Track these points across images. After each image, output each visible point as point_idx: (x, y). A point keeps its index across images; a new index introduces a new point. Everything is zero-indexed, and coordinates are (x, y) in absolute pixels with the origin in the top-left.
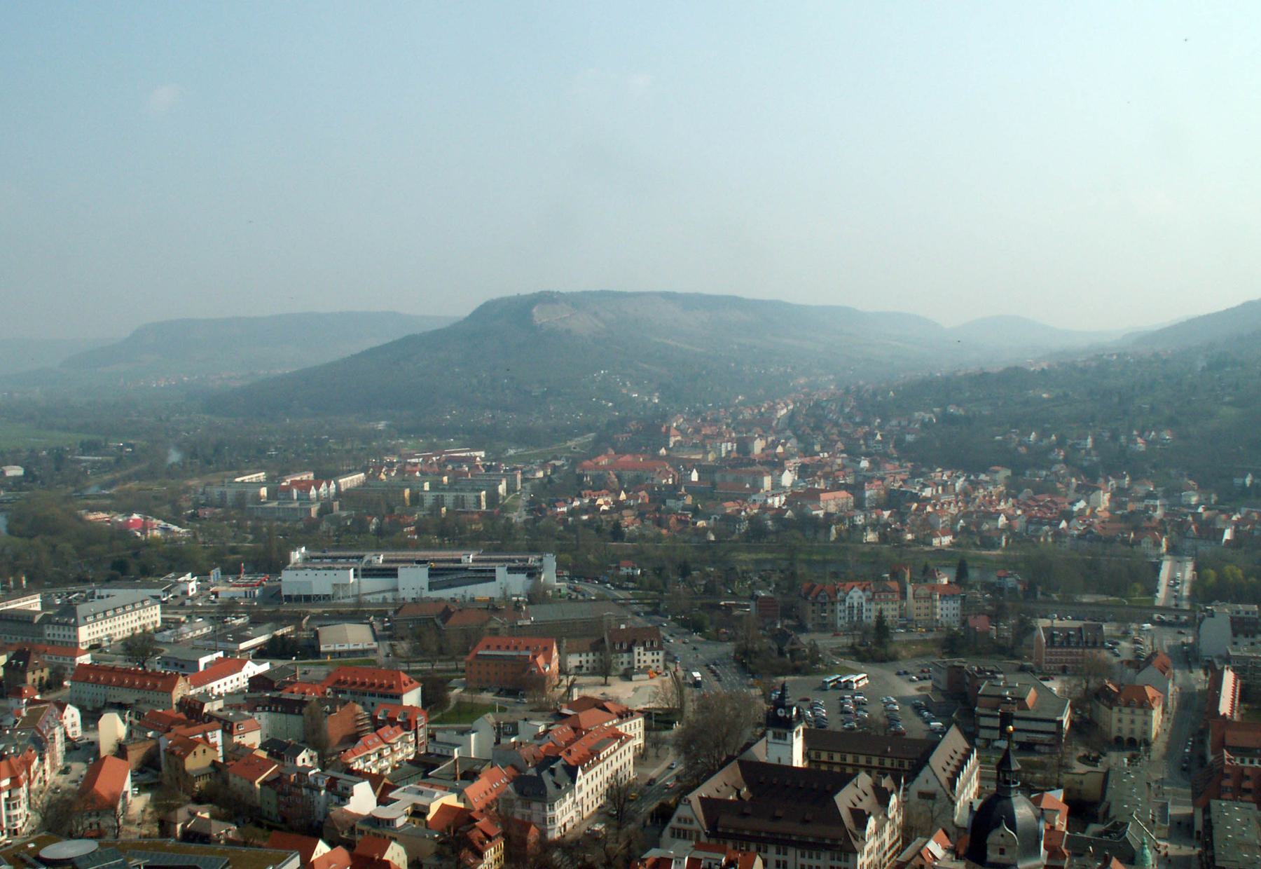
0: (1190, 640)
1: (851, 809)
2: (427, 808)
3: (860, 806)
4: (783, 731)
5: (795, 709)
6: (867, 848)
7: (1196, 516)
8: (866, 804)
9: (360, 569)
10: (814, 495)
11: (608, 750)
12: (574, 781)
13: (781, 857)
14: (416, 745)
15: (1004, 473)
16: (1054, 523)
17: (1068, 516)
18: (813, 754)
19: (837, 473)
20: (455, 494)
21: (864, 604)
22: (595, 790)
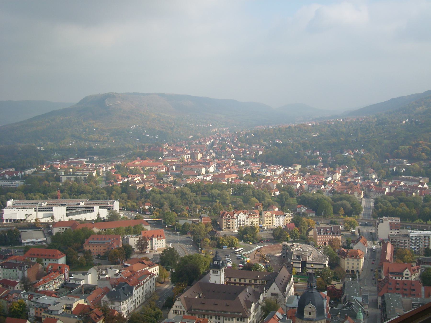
0: (374, 231)
1: (245, 301)
2: (72, 305)
3: (248, 299)
4: (216, 270)
6: (252, 316)
7: (374, 183)
8: (250, 299)
9: (37, 208)
10: (223, 176)
11: (145, 280)
12: (132, 293)
14: (65, 280)
15: (298, 167)
16: (319, 186)
17: (325, 183)
18: (228, 279)
19: (231, 167)
20: (75, 176)
21: (245, 219)
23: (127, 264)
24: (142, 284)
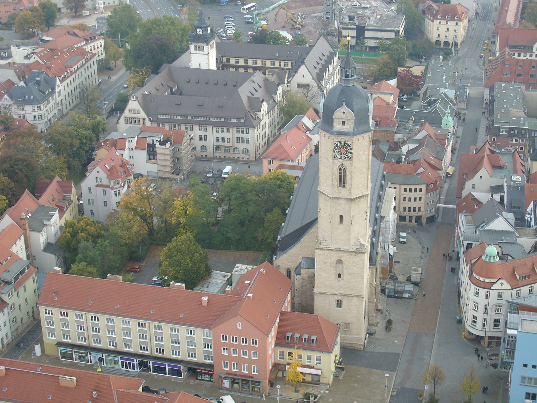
3: (256, 95)
4: (201, 45)
5: (209, 28)
6: (262, 124)
11: (78, 65)
12: (53, 89)
13: (203, 133)
22: (70, 93)
23: (45, 38)
24: (71, 73)
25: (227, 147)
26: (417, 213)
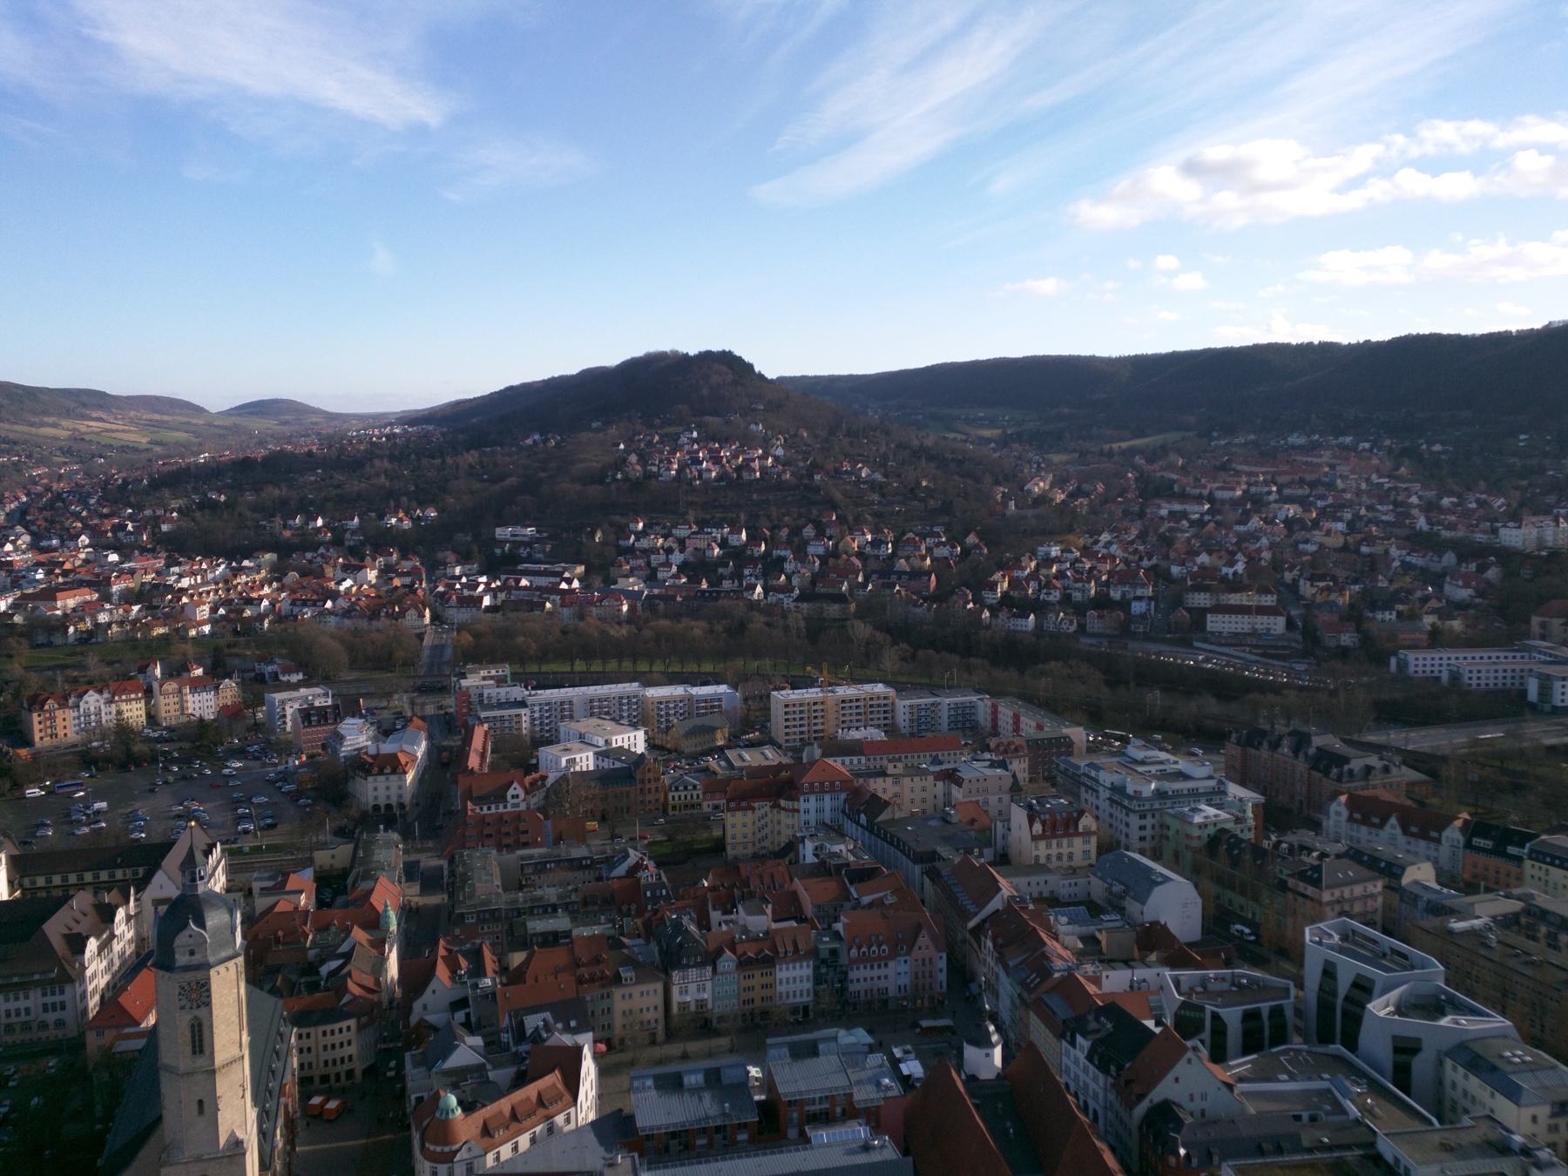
25: (25, 1023)
26: (347, 1066)
